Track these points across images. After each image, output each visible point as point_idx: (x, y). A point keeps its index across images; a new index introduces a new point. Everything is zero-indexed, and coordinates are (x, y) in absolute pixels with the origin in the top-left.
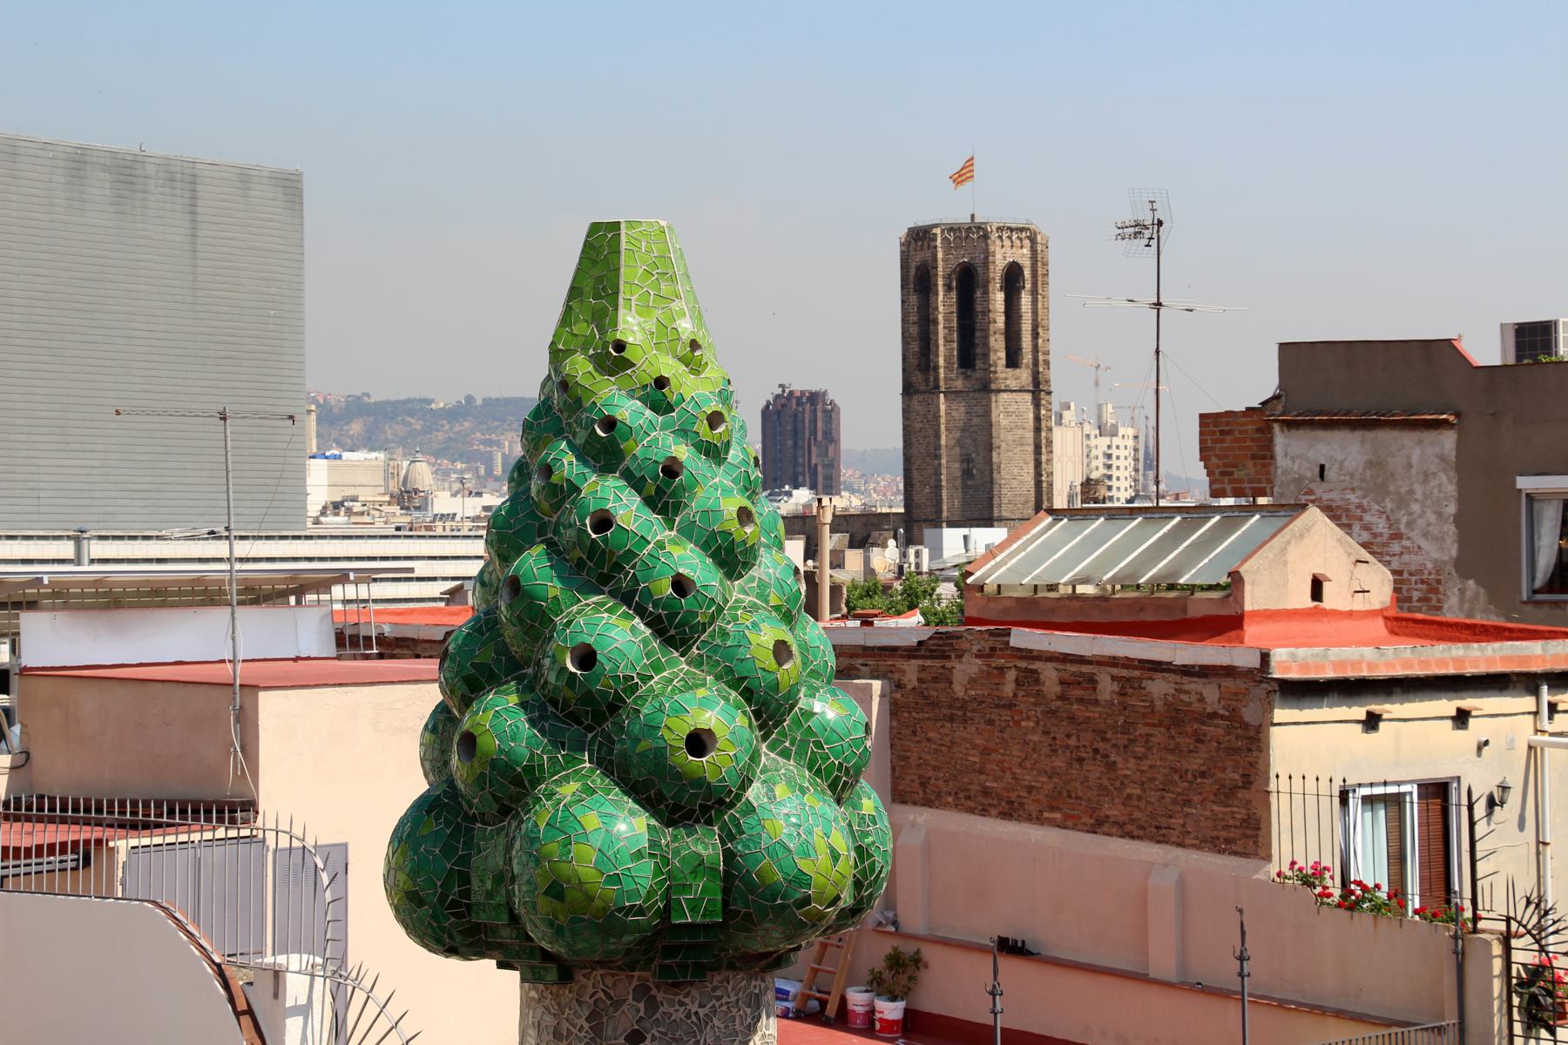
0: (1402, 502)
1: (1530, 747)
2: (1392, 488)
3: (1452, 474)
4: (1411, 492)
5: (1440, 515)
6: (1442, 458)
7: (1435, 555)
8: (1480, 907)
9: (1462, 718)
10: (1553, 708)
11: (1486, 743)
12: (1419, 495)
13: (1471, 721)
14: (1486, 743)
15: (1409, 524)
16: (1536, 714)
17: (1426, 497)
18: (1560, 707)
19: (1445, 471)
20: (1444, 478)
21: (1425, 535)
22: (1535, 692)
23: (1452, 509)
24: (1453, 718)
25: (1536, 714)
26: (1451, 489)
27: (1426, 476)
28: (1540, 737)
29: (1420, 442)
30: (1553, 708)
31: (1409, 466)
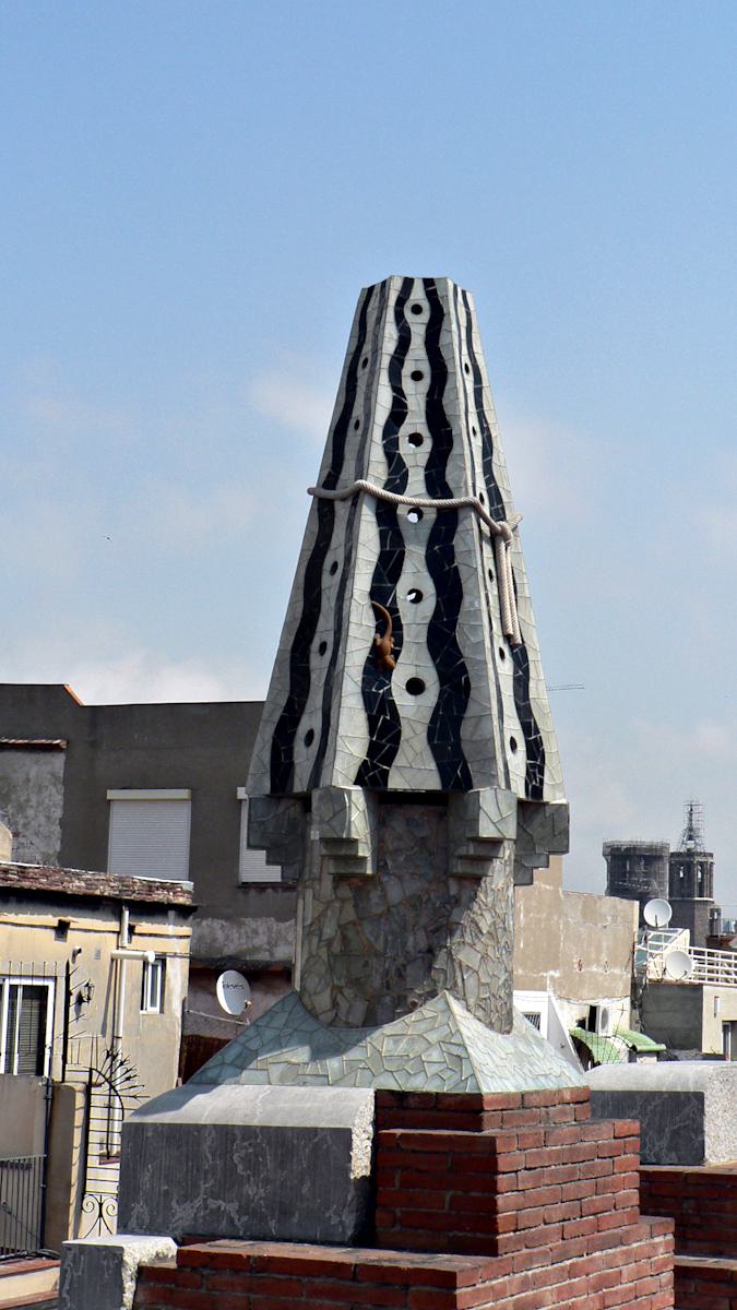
0: (21, 808)
1: (112, 960)
2: (13, 797)
3: (60, 786)
4: (28, 800)
5: (48, 818)
6: (53, 775)
7: (43, 850)
8: (69, 1061)
9: (62, 929)
10: (131, 929)
11: (80, 951)
12: (34, 801)
13: (69, 931)
14: (80, 951)
15: (25, 825)
16: (119, 933)
17: (39, 804)
18: (137, 931)
19: (55, 785)
20: (54, 790)
21: (37, 834)
22: (120, 919)
23: (58, 813)
24: (54, 928)
25: (119, 933)
26: (59, 798)
27: (40, 789)
28: (121, 952)
29: (37, 762)
30: (131, 929)
31: (28, 780)
